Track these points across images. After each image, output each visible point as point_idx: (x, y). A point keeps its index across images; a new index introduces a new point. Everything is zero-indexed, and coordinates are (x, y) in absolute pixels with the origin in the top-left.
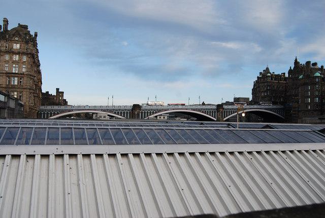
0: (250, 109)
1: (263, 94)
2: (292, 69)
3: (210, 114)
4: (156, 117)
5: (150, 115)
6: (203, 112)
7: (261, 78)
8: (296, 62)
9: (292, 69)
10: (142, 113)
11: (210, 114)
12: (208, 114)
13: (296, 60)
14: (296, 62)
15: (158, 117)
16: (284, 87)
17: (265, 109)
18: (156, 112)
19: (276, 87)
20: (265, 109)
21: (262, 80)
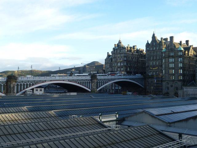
0: (119, 79)
1: (119, 64)
2: (150, 42)
3: (85, 85)
4: (33, 89)
5: (27, 88)
6: (79, 83)
7: (117, 49)
8: (154, 37)
9: (150, 42)
10: (18, 85)
11: (85, 85)
12: (83, 85)
13: (154, 35)
14: (154, 37)
15: (35, 90)
16: (137, 58)
17: (130, 79)
18: (33, 85)
19: (130, 58)
20: (130, 79)
21: (119, 51)
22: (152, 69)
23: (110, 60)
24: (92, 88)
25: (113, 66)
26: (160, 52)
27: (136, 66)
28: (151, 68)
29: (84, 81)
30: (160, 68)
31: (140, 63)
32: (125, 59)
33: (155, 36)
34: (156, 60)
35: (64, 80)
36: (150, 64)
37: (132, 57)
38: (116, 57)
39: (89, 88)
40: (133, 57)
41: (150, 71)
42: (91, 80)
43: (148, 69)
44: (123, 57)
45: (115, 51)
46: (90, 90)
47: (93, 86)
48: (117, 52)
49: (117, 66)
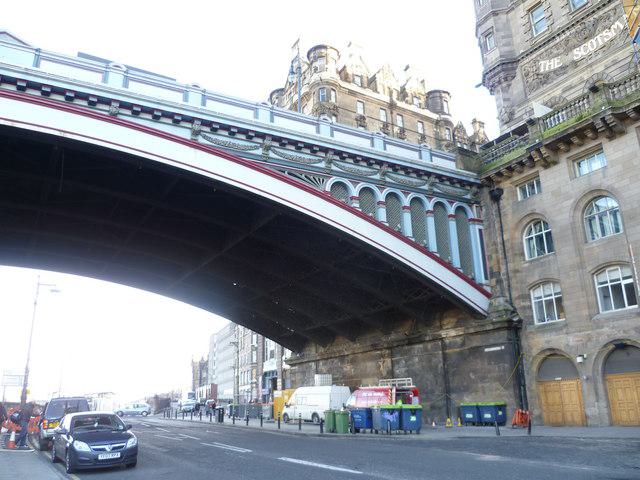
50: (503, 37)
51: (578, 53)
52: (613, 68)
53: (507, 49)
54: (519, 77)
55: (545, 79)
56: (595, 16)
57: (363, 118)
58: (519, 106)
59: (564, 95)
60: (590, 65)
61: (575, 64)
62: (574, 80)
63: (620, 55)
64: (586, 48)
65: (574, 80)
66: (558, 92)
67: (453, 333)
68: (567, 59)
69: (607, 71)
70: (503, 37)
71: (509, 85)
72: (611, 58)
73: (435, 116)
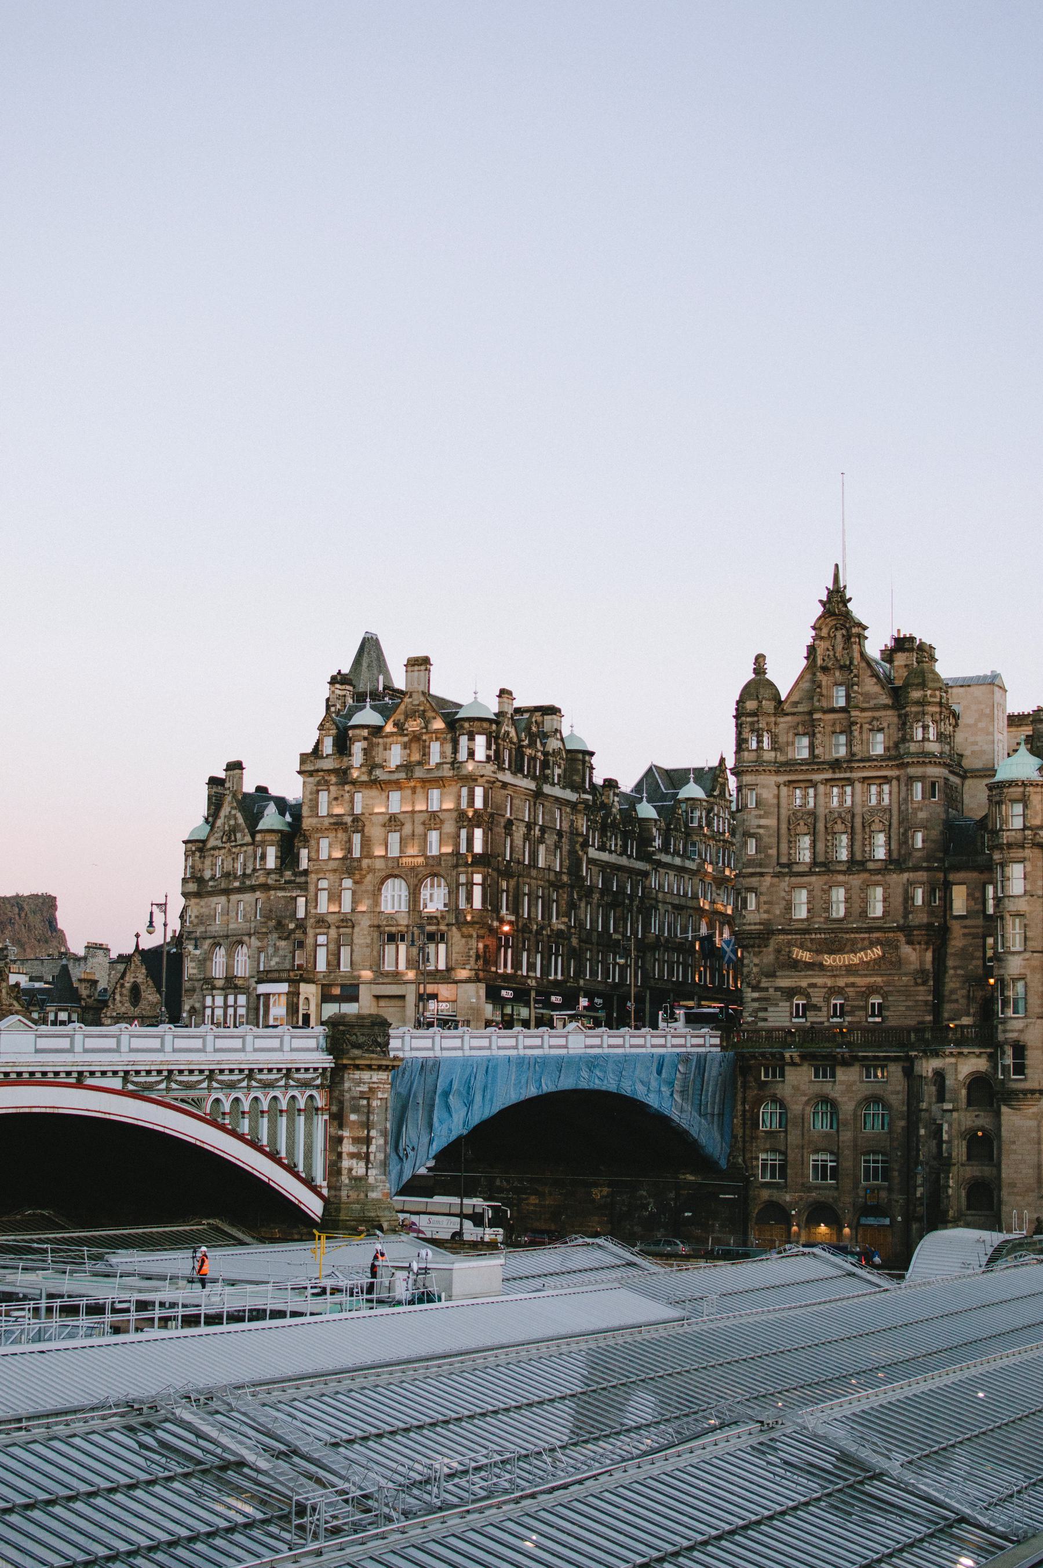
22: (810, 966)
23: (272, 852)
24: (333, 1170)
25: (321, 922)
26: (911, 780)
27: (557, 923)
28: (806, 956)
29: (267, 1085)
30: (906, 950)
31: (591, 889)
32: (478, 848)
33: (857, 609)
34: (857, 864)
35: (79, 1081)
36: (789, 907)
37: (529, 826)
38: (358, 823)
39: (308, 1183)
40: (543, 830)
41: (784, 983)
42: (333, 1079)
43: (768, 957)
44: (449, 827)
45: (342, 746)
46: (314, 1206)
47: (347, 1147)
48: (371, 764)
49: (365, 922)
50: (765, 903)
51: (828, 960)
52: (852, 989)
53: (765, 916)
54: (771, 949)
55: (795, 965)
56: (848, 936)
57: (510, 823)
58: (767, 976)
59: (810, 990)
60: (835, 976)
61: (821, 966)
62: (819, 981)
63: (859, 981)
64: (834, 961)
65: (819, 981)
66: (804, 984)
67: (690, 1178)
68: (818, 958)
69: (847, 989)
70: (765, 903)
71: (761, 952)
72: (852, 980)
73: (571, 796)
